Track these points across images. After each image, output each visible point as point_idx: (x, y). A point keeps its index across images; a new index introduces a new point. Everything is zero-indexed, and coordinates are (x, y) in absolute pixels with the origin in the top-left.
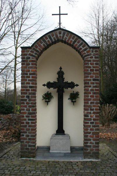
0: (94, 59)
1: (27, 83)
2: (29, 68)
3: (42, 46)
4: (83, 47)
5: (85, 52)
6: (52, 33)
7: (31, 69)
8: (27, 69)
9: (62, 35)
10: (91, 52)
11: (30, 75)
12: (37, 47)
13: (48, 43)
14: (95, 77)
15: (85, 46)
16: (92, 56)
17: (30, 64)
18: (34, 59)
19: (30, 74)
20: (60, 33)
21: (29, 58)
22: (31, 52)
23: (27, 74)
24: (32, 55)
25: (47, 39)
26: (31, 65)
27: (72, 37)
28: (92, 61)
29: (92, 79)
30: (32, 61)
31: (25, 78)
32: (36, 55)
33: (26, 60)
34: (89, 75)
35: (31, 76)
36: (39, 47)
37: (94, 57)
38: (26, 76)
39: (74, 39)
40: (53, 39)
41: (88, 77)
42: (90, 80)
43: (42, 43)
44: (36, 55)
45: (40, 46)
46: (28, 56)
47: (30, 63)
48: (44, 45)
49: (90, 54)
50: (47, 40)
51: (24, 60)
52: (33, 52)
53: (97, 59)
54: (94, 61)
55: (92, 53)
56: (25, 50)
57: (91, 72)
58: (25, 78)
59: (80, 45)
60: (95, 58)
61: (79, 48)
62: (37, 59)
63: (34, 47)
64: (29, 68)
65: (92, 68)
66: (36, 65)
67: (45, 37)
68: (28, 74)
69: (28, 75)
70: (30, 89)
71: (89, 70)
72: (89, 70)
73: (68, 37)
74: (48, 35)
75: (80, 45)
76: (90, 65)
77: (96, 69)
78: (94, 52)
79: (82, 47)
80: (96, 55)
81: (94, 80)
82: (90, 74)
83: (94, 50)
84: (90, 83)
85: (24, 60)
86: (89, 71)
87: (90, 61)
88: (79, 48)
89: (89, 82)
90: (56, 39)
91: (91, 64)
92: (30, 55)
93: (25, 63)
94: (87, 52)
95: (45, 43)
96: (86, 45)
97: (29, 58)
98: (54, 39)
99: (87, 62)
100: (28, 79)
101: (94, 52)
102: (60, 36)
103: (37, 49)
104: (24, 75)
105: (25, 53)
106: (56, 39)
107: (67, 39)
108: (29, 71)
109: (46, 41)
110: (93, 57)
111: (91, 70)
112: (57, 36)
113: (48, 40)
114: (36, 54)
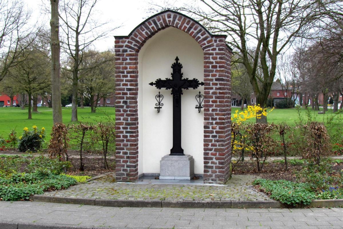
0: (217, 51)
1: (124, 85)
2: (126, 64)
3: (144, 35)
4: (202, 35)
5: (205, 42)
6: (157, 17)
7: (128, 66)
8: (123, 66)
9: (171, 19)
10: (213, 42)
11: (127, 73)
12: (136, 36)
13: (152, 30)
14: (219, 76)
15: (205, 34)
16: (215, 47)
17: (127, 59)
18: (133, 53)
19: (128, 72)
20: (169, 17)
21: (126, 51)
22: (128, 42)
23: (123, 72)
24: (130, 47)
25: (150, 24)
26: (128, 61)
27: (187, 21)
28: (214, 55)
29: (214, 78)
30: (131, 55)
31: (120, 77)
32: (136, 47)
33: (121, 53)
34: (211, 74)
35: (129, 75)
36: (140, 36)
37: (217, 48)
38: (121, 75)
39: (190, 25)
40: (159, 25)
41: (209, 76)
42: (212, 80)
43: (144, 30)
44: (136, 47)
45: (141, 34)
46: (124, 48)
47: (128, 58)
48: (146, 33)
49: (213, 45)
50: (150, 27)
51: (119, 53)
52: (131, 43)
53: (222, 52)
54: (217, 54)
55: (215, 44)
56: (121, 40)
57: (213, 69)
58: (120, 77)
59: (198, 33)
60: (219, 50)
61: (197, 37)
62: (138, 51)
63: (133, 36)
64: (126, 64)
65: (214, 64)
66: (136, 59)
67: (148, 22)
68: (125, 72)
69: (125, 74)
70: (128, 92)
71: (211, 67)
72: (211, 67)
73: (180, 21)
74: (153, 19)
75: (198, 33)
76: (211, 60)
77: (220, 65)
78: (218, 42)
79: (200, 36)
80: (221, 46)
81: (216, 80)
82: (212, 71)
83: (218, 40)
84: (211, 85)
85: (119, 53)
86: (211, 68)
87: (212, 54)
88: (197, 37)
89: (210, 83)
90: (164, 25)
91: (213, 58)
92: (128, 47)
93: (121, 58)
94: (208, 42)
95: (148, 31)
96: (206, 33)
97: (126, 51)
98: (161, 25)
99: (207, 56)
100: (125, 79)
101: (218, 42)
102: (170, 21)
103: (137, 39)
104: (120, 74)
105: (121, 44)
106: (164, 25)
107: (180, 24)
108: (126, 68)
109: (149, 28)
110: (216, 49)
111: (213, 67)
112: (164, 20)
113: (152, 26)
114: (135, 45)
